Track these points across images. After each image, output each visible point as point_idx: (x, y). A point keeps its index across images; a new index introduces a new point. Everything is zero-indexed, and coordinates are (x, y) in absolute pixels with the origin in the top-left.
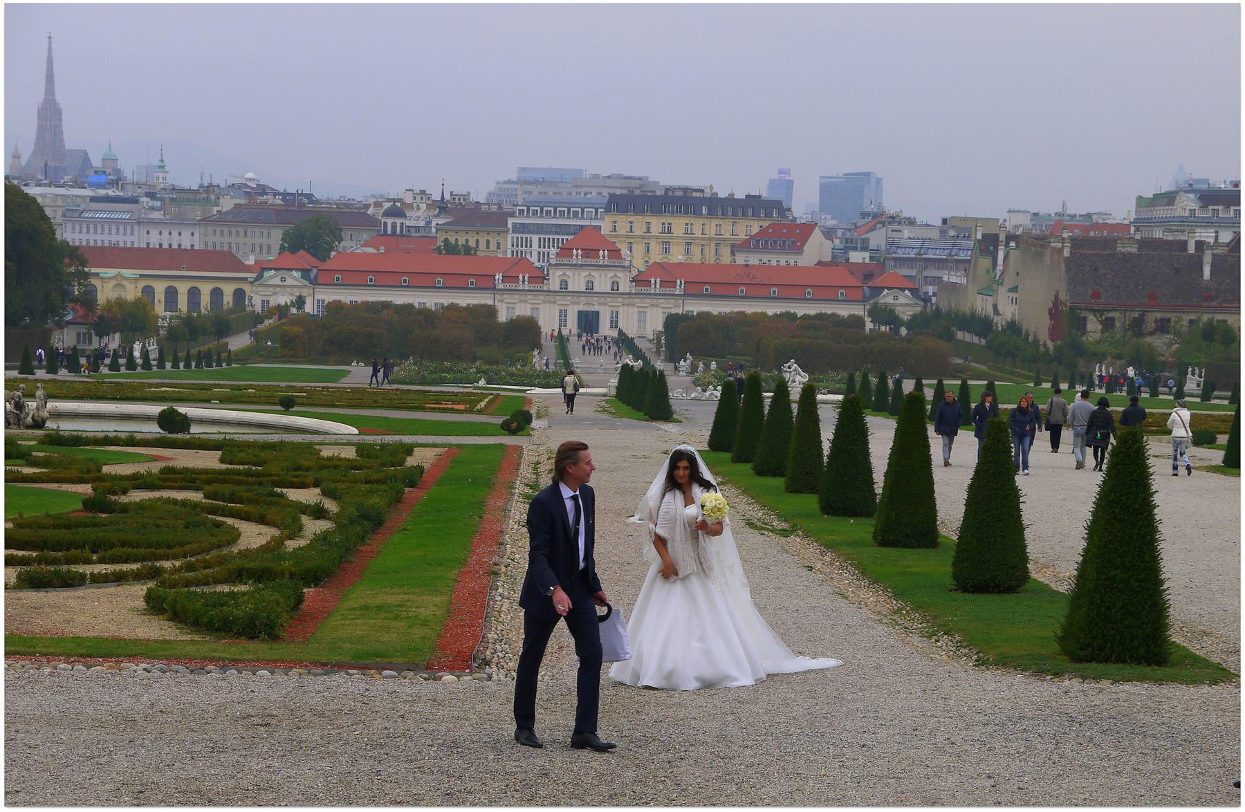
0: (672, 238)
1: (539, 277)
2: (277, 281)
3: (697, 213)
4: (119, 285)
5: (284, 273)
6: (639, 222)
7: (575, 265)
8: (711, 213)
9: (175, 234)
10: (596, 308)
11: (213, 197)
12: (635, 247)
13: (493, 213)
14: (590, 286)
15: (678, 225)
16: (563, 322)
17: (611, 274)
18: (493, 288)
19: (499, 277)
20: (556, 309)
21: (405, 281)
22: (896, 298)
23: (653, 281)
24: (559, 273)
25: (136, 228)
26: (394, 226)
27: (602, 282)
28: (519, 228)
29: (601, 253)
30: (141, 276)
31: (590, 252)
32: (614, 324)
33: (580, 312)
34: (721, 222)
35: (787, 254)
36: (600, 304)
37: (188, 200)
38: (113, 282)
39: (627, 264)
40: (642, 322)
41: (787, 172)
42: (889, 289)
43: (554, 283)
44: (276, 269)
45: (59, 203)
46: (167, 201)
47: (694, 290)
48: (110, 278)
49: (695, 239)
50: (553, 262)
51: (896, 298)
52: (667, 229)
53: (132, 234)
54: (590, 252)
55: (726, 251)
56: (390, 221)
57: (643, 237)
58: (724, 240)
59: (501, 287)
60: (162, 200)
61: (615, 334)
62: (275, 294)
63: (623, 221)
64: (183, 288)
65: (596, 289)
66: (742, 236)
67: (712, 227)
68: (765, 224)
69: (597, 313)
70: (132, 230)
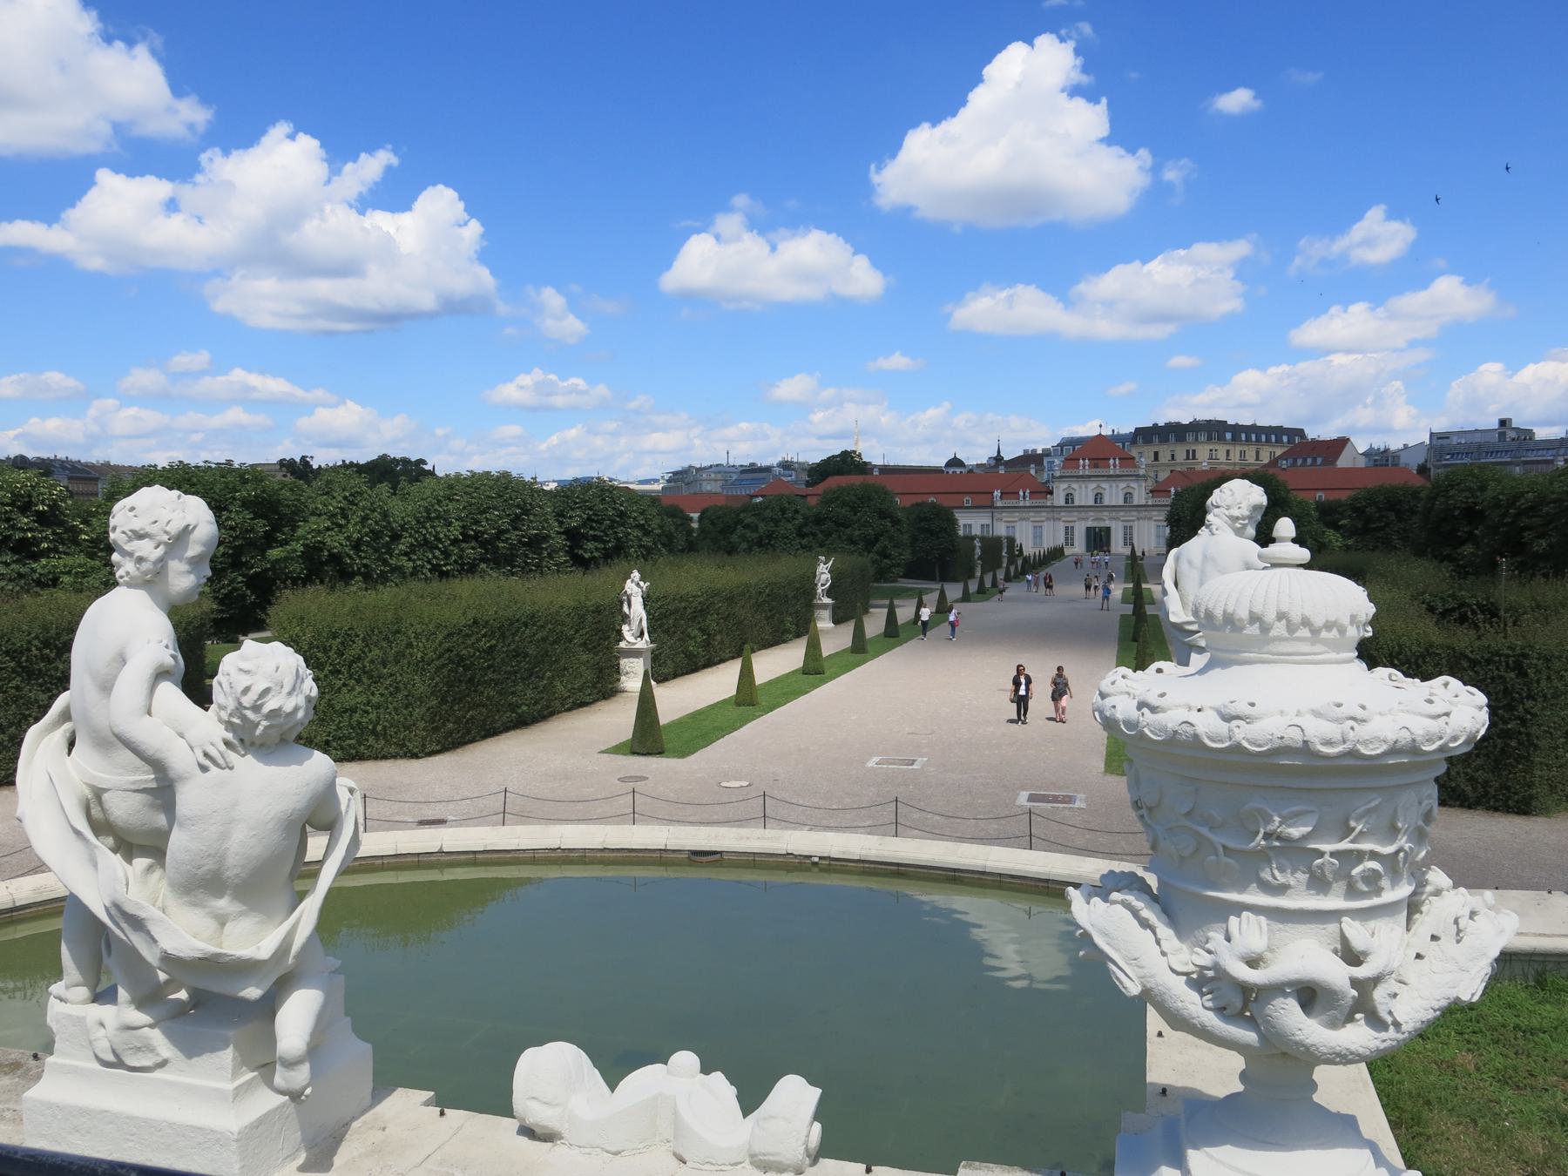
3: (1221, 439)
8: (1236, 439)
10: (1107, 524)
14: (1098, 497)
17: (1122, 485)
18: (992, 506)
19: (997, 493)
20: (1061, 527)
24: (1064, 486)
27: (1113, 494)
31: (1098, 461)
32: (1128, 540)
36: (1111, 519)
43: (1059, 498)
54: (1098, 461)
59: (999, 504)
61: (1127, 551)
66: (1266, 461)
69: (1108, 529)
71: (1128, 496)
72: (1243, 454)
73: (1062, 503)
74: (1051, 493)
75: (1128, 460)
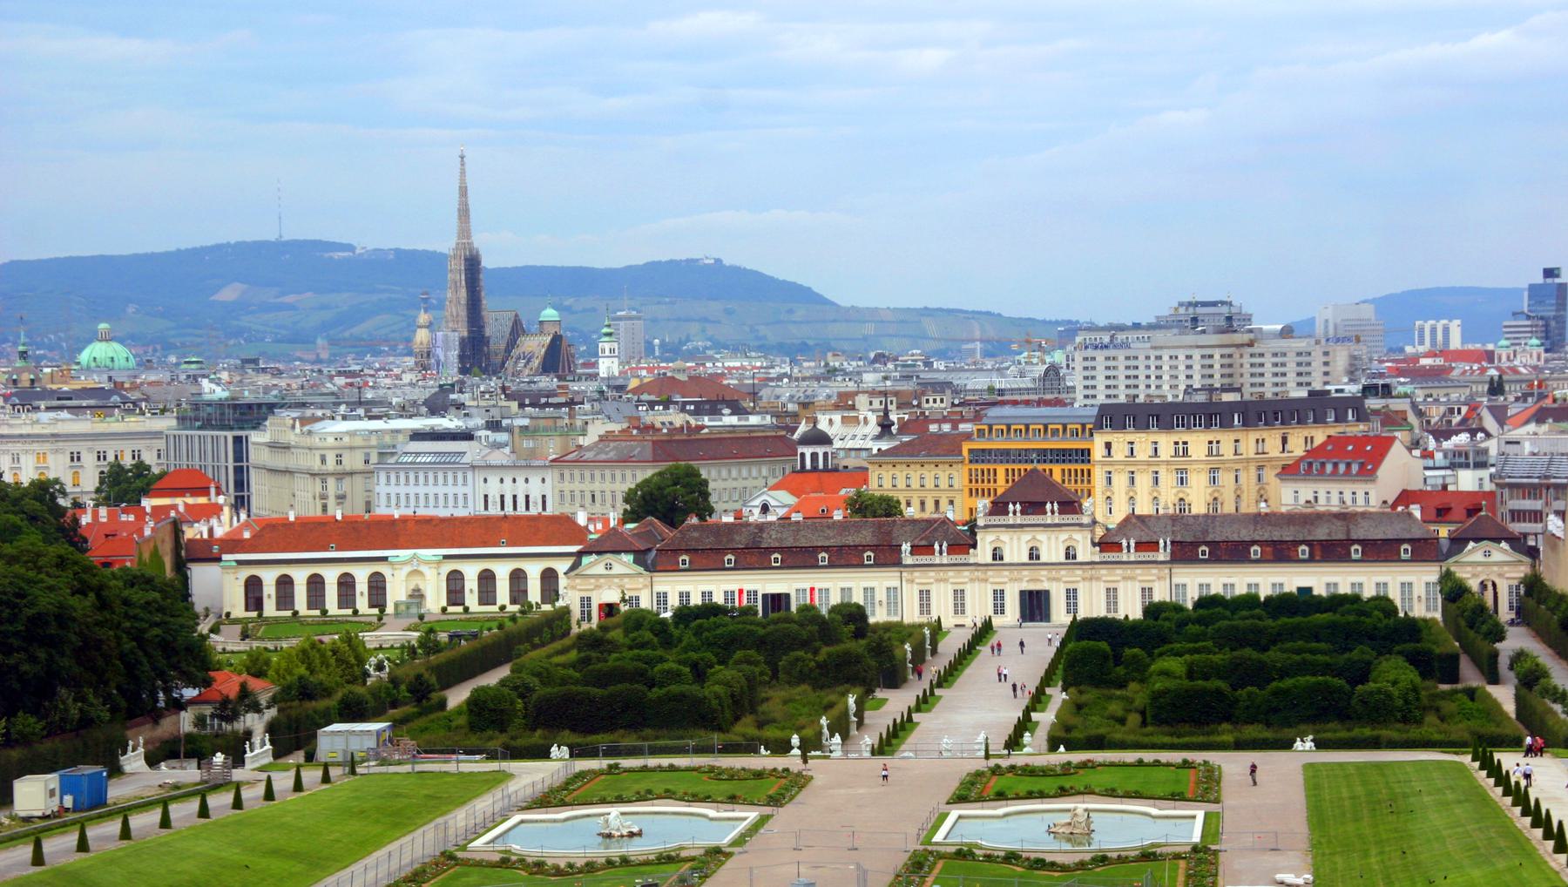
1: (963, 541)
2: (600, 569)
3: (1226, 424)
4: (416, 572)
5: (609, 558)
6: (1143, 441)
8: (1246, 424)
9: (520, 480)
11: (579, 423)
12: (1137, 477)
13: (945, 435)
14: (1034, 554)
15: (1197, 442)
16: (999, 609)
17: (1063, 536)
19: (906, 547)
21: (776, 560)
22: (1487, 554)
25: (470, 475)
26: (814, 456)
27: (1052, 547)
28: (978, 456)
29: (1048, 506)
30: (446, 557)
31: (1033, 507)
32: (1072, 606)
33: (1022, 593)
35: (1354, 481)
37: (546, 429)
38: (408, 569)
39: (1086, 520)
41: (1549, 273)
42: (1477, 540)
43: (983, 553)
44: (599, 553)
45: (374, 442)
46: (517, 431)
47: (1184, 553)
48: (405, 563)
49: (1223, 462)
51: (1487, 554)
52: (1182, 450)
53: (465, 483)
55: (1270, 475)
56: (808, 451)
57: (1149, 464)
58: (1271, 460)
60: (509, 430)
62: (598, 587)
63: (1120, 440)
64: (502, 571)
65: (1043, 559)
67: (1249, 441)
69: (1047, 592)
70: (465, 478)
71: (1070, 554)
73: (989, 560)
74: (974, 546)
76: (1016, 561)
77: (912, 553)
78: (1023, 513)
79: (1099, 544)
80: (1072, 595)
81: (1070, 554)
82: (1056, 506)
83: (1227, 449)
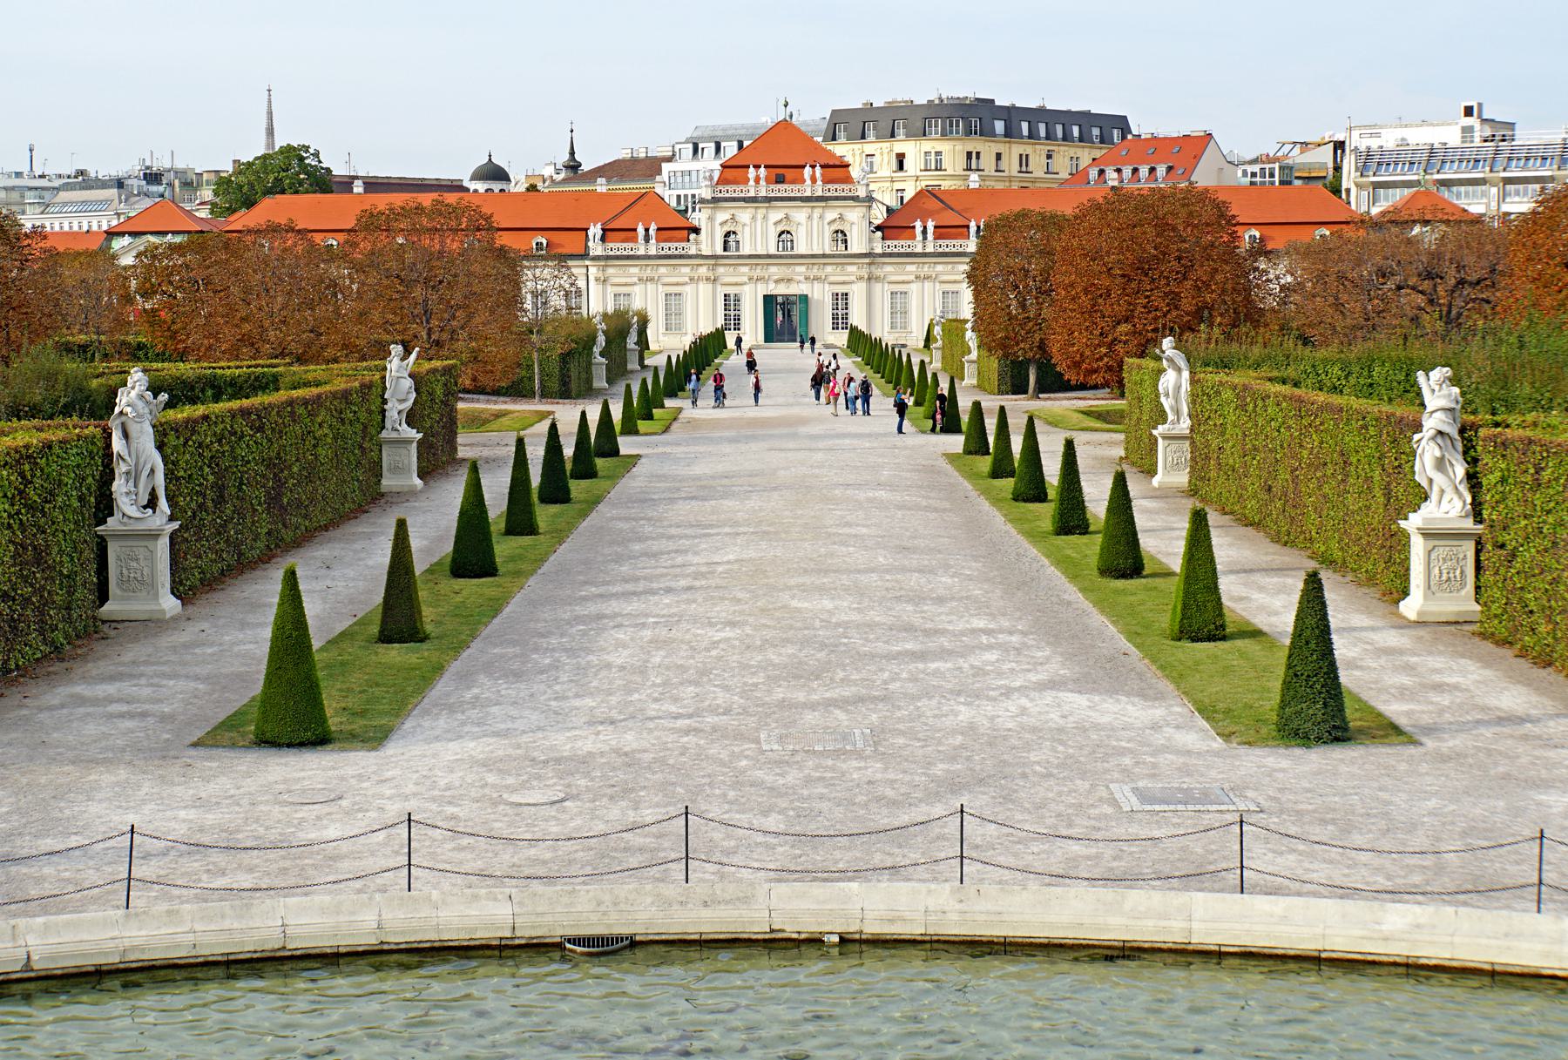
0: (944, 178)
3: (987, 132)
7: (754, 200)
8: (1009, 133)
19: (595, 231)
23: (918, 225)
24: (722, 216)
27: (812, 231)
32: (840, 320)
33: (769, 300)
34: (1028, 149)
40: (899, 313)
43: (709, 242)
50: (706, 194)
61: (842, 338)
66: (1064, 175)
68: (1098, 154)
69: (804, 299)
72: (1024, 160)
73: (719, 251)
75: (837, 170)
76: (760, 252)
77: (603, 239)
78: (768, 181)
79: (878, 228)
80: (842, 299)
81: (841, 236)
82: (818, 170)
83: (988, 162)
